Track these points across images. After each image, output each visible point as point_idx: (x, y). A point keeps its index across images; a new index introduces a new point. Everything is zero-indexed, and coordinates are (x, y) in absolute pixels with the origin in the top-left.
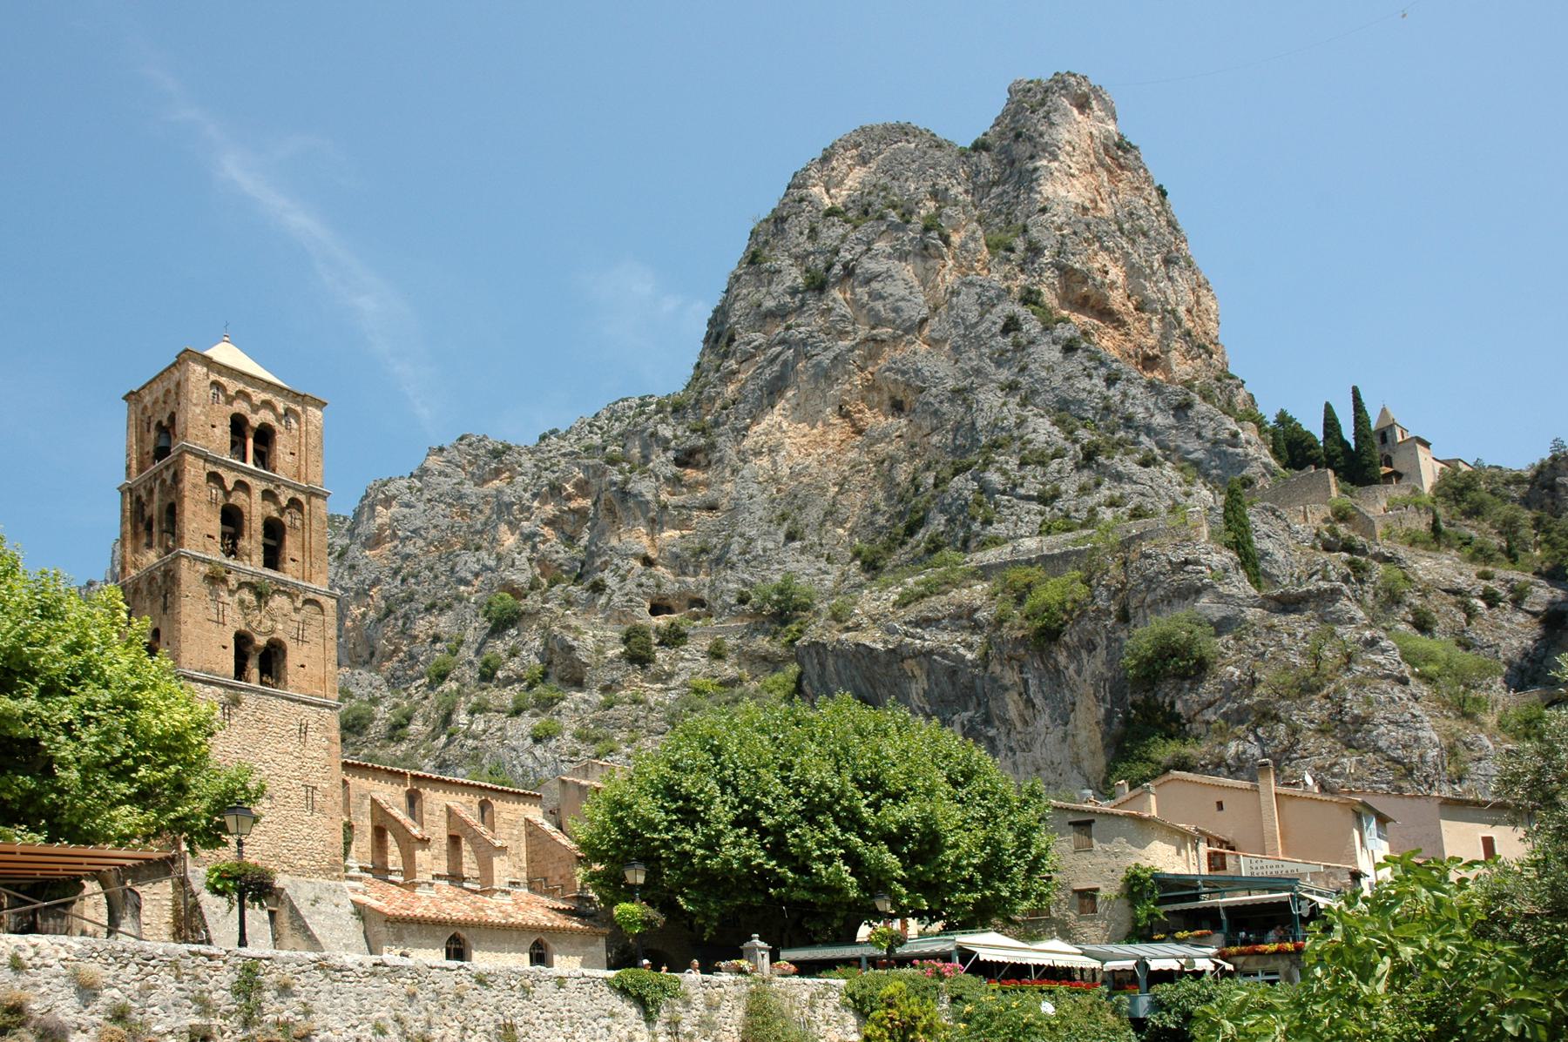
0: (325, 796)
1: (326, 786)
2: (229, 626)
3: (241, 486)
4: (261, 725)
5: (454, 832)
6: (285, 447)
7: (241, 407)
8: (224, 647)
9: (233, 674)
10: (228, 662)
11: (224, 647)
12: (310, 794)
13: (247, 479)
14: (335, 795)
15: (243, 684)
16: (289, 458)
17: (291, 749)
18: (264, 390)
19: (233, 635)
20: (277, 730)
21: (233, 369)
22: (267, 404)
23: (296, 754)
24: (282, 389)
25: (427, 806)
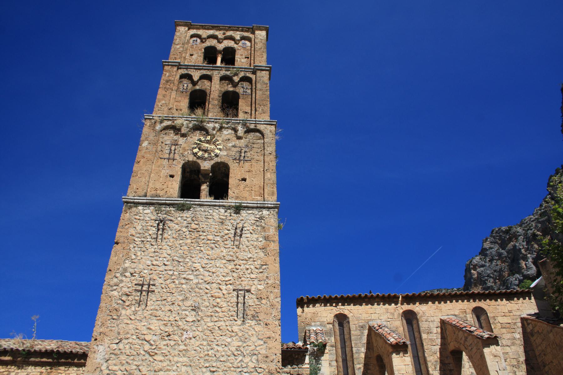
0: (260, 299)
1: (260, 287)
4: (195, 235)
5: (452, 346)
6: (242, 55)
7: (212, 42)
8: (172, 176)
10: (175, 186)
11: (172, 176)
12: (241, 299)
14: (272, 296)
17: (224, 254)
19: (181, 166)
20: (211, 237)
25: (423, 325)
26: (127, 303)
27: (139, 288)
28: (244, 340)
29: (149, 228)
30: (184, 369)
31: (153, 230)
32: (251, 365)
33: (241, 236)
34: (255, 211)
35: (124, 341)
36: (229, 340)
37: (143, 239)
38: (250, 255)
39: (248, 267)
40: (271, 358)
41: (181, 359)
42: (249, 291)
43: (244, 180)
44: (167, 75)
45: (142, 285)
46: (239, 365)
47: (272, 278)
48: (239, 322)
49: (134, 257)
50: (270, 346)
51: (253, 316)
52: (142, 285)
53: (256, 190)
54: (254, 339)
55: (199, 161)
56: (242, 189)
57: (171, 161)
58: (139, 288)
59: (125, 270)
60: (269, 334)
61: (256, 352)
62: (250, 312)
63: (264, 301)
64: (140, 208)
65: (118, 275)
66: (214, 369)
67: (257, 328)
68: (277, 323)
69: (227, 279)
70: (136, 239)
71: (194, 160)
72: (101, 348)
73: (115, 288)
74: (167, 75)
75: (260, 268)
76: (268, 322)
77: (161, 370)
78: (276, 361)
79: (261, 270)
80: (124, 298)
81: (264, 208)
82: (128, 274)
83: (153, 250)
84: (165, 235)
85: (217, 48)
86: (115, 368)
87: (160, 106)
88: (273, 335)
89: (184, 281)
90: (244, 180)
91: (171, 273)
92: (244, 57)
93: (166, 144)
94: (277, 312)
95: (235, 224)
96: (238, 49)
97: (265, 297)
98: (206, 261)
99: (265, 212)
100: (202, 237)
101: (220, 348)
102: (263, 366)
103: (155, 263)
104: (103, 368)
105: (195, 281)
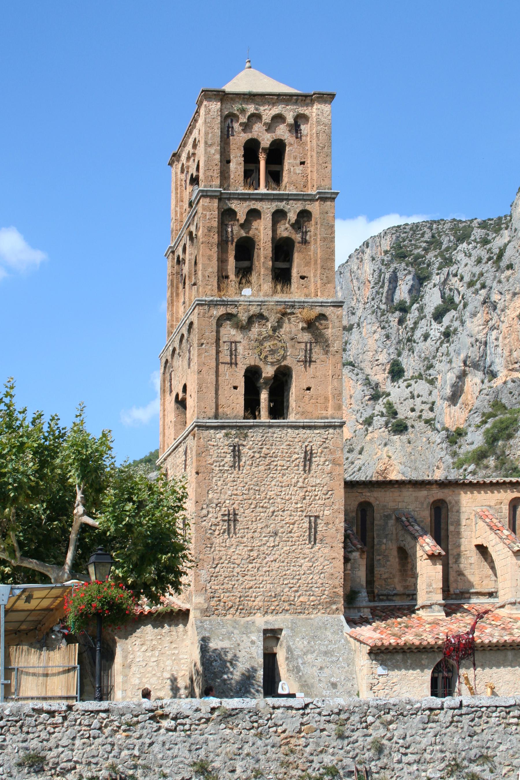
0: (327, 524)
1: (326, 513)
2: (240, 365)
3: (254, 214)
6: (295, 158)
8: (235, 388)
9: (242, 413)
11: (235, 388)
13: (258, 205)
14: (337, 521)
15: (251, 422)
16: (299, 169)
17: (294, 481)
18: (274, 104)
19: (243, 372)
21: (244, 94)
22: (279, 118)
23: (300, 484)
24: (291, 95)
26: (217, 532)
27: (226, 518)
28: (313, 560)
29: (225, 454)
30: (268, 586)
31: (229, 458)
32: (320, 581)
33: (310, 460)
34: (322, 431)
35: (219, 566)
36: (302, 561)
37: (221, 468)
38: (318, 481)
39: (316, 493)
40: (336, 576)
41: (265, 578)
42: (317, 517)
43: (309, 389)
44: (208, 217)
45: (229, 514)
46: (310, 582)
47: (337, 503)
48: (310, 546)
49: (216, 488)
50: (335, 566)
51: (321, 540)
52: (229, 514)
53: (321, 402)
54: (321, 560)
55: (261, 364)
56: (307, 402)
57: (233, 366)
58: (226, 518)
59: (211, 501)
60: (335, 555)
61: (324, 571)
62: (318, 537)
63: (330, 526)
64: (212, 431)
65: (205, 506)
66: (292, 586)
67: (326, 550)
68: (342, 545)
69: (299, 505)
70: (215, 468)
71: (256, 364)
72: (203, 572)
73: (204, 518)
74: (208, 217)
75: (327, 494)
76: (333, 545)
77: (251, 588)
78: (339, 578)
79: (328, 496)
80: (213, 528)
81: (330, 427)
82: (214, 505)
83: (232, 479)
84: (242, 463)
85: (262, 142)
86: (217, 587)
87: (207, 278)
88: (338, 556)
89: (261, 510)
90: (309, 389)
91: (250, 501)
92: (298, 162)
93: (224, 342)
94: (341, 537)
95: (304, 446)
96: (291, 145)
97: (331, 522)
98: (279, 489)
99: (331, 431)
100: (275, 463)
101: (295, 568)
102: (330, 582)
103: (235, 492)
104: (208, 588)
105: (272, 509)
